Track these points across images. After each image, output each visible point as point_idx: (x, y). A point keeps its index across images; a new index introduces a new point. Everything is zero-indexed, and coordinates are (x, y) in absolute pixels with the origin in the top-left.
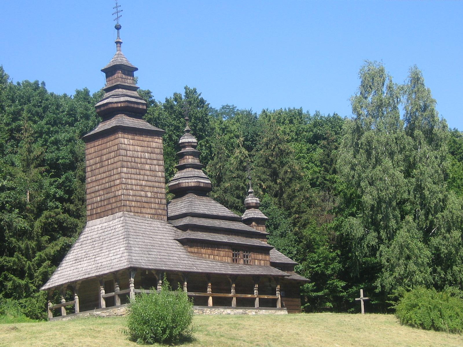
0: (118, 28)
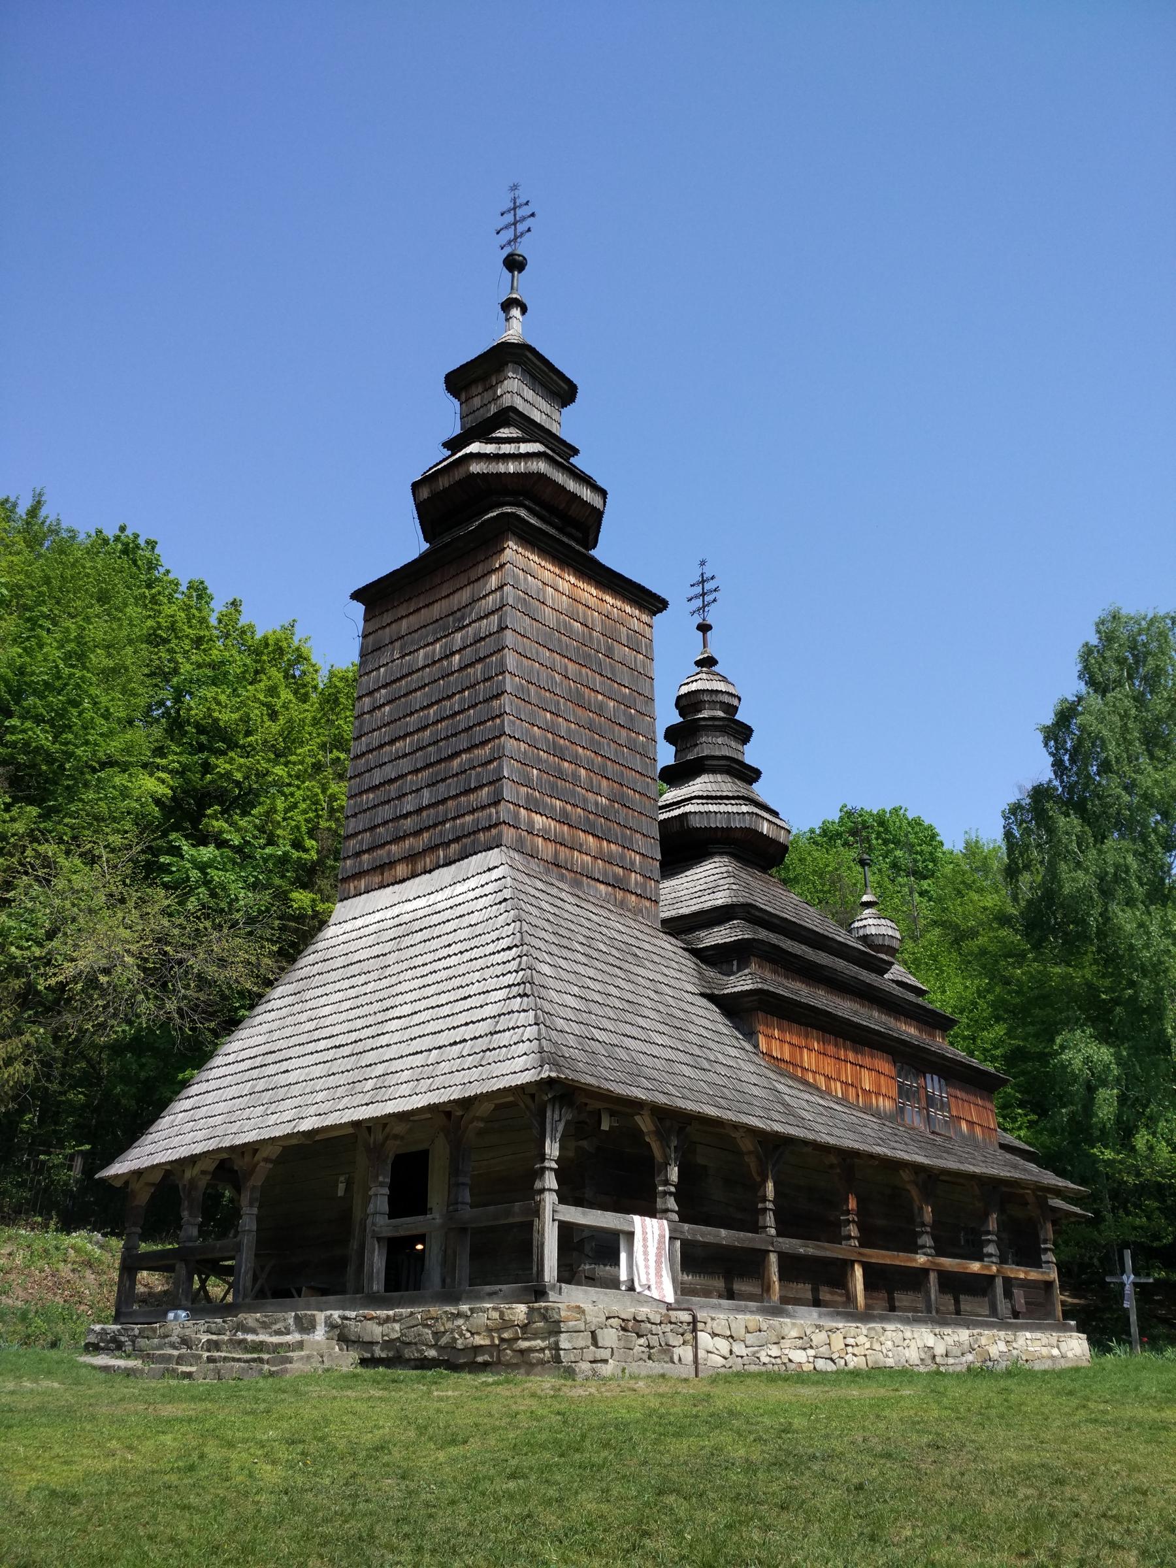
0: (514, 264)
